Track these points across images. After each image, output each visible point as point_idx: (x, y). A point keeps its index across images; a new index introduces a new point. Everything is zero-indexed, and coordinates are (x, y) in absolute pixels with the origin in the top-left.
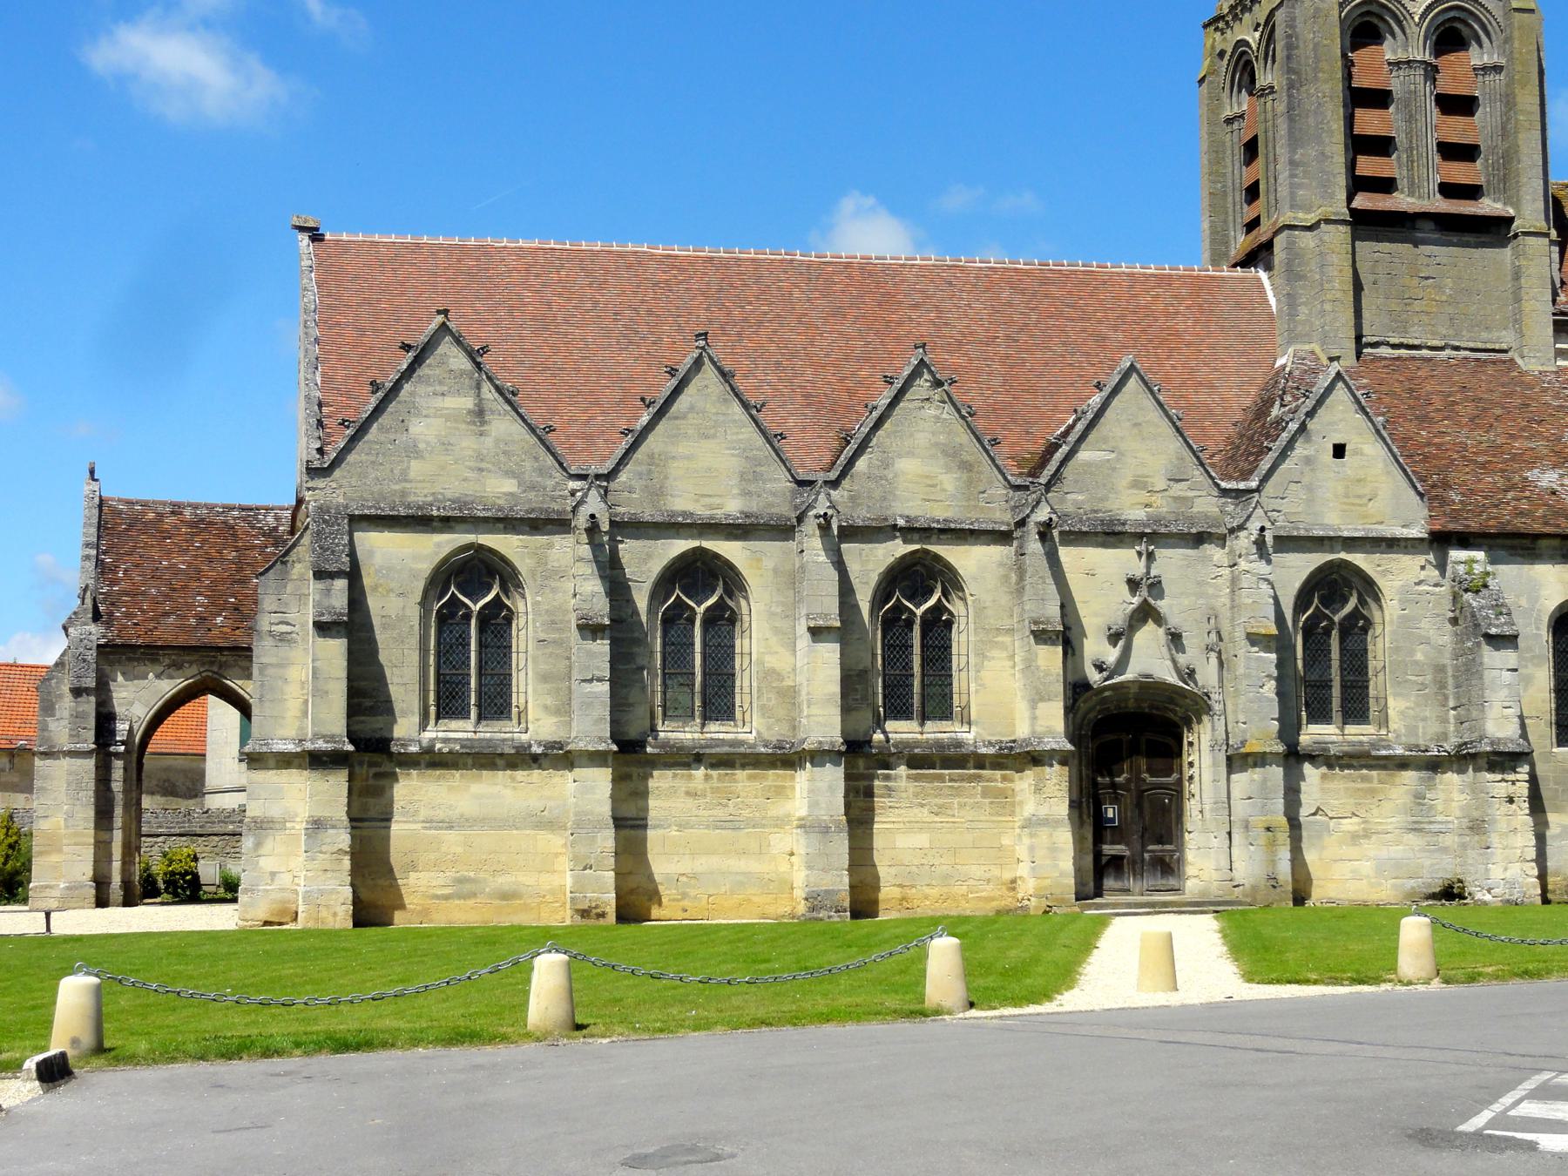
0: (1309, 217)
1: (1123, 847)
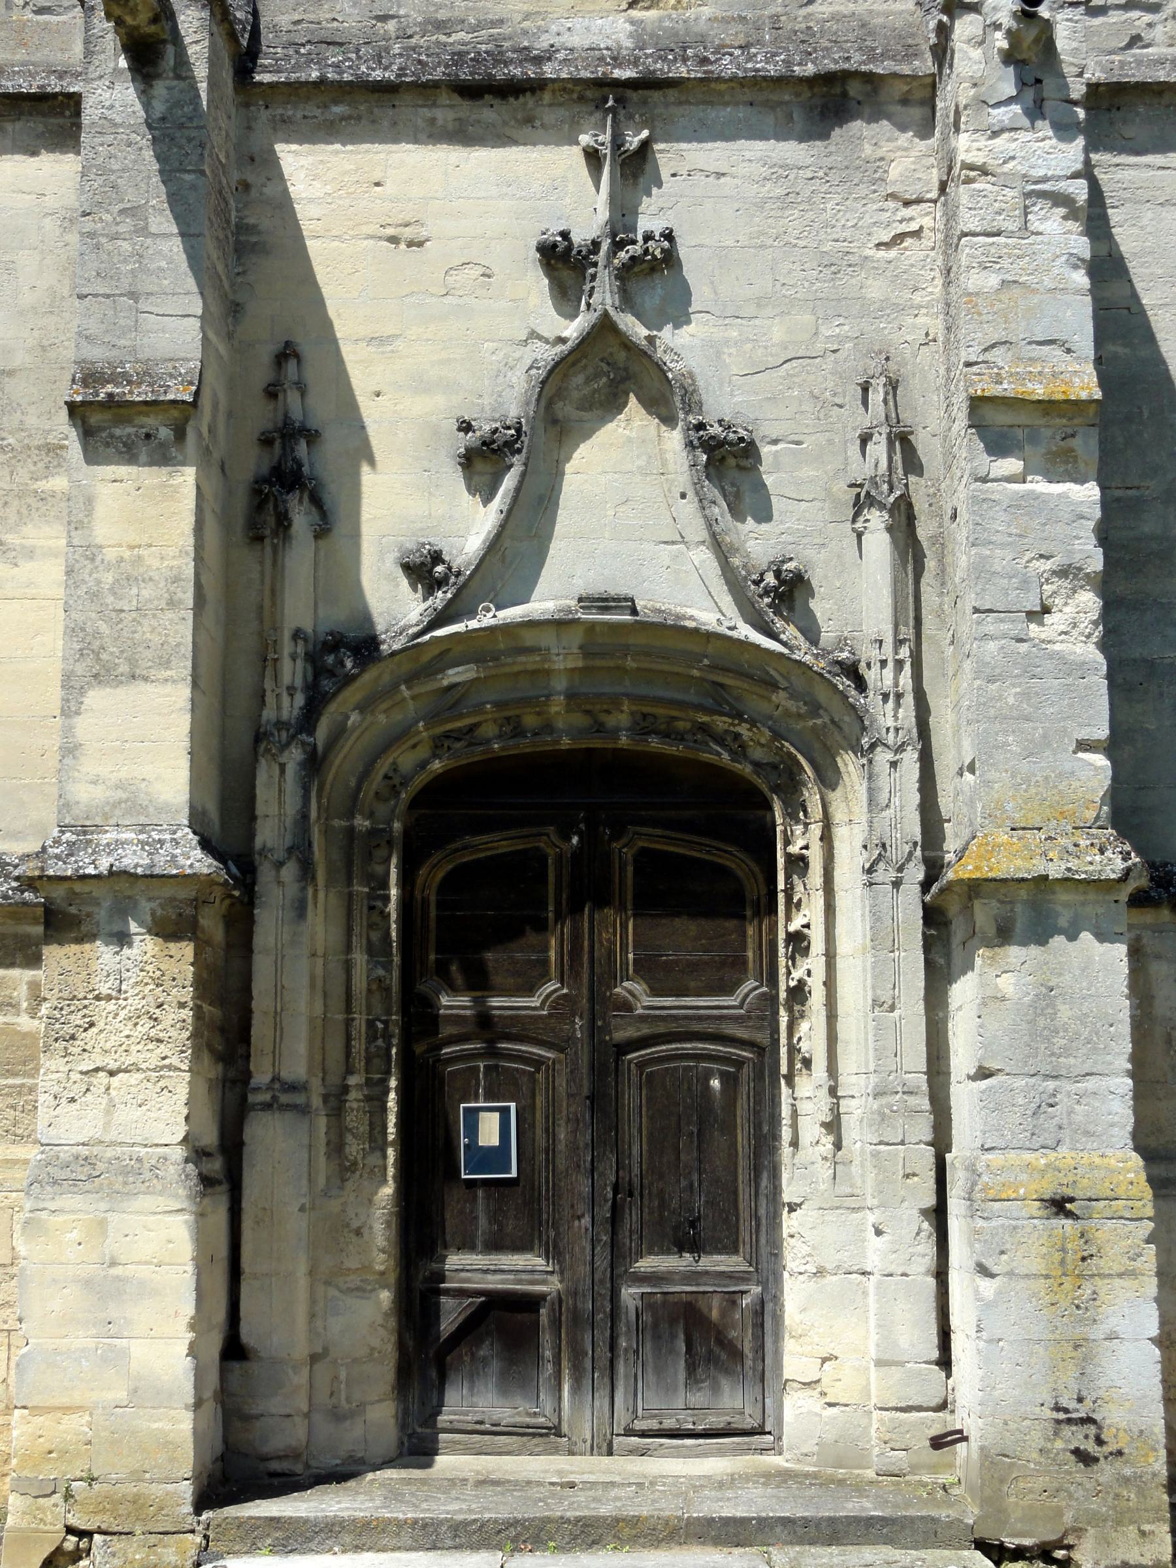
1: (534, 1261)
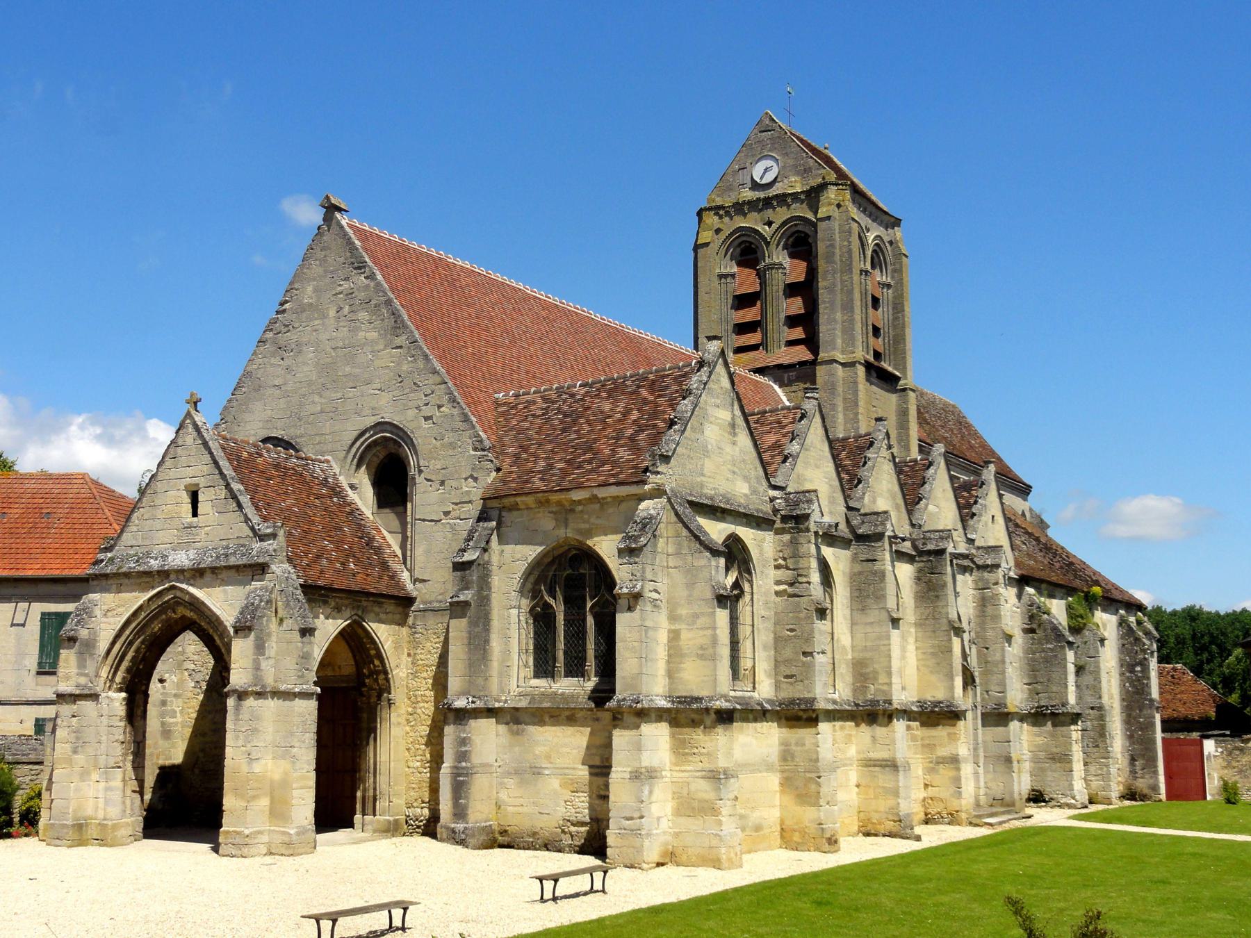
0: (841, 356)
